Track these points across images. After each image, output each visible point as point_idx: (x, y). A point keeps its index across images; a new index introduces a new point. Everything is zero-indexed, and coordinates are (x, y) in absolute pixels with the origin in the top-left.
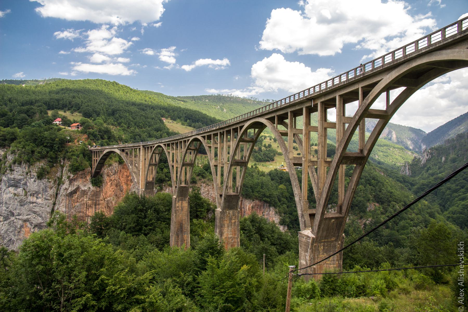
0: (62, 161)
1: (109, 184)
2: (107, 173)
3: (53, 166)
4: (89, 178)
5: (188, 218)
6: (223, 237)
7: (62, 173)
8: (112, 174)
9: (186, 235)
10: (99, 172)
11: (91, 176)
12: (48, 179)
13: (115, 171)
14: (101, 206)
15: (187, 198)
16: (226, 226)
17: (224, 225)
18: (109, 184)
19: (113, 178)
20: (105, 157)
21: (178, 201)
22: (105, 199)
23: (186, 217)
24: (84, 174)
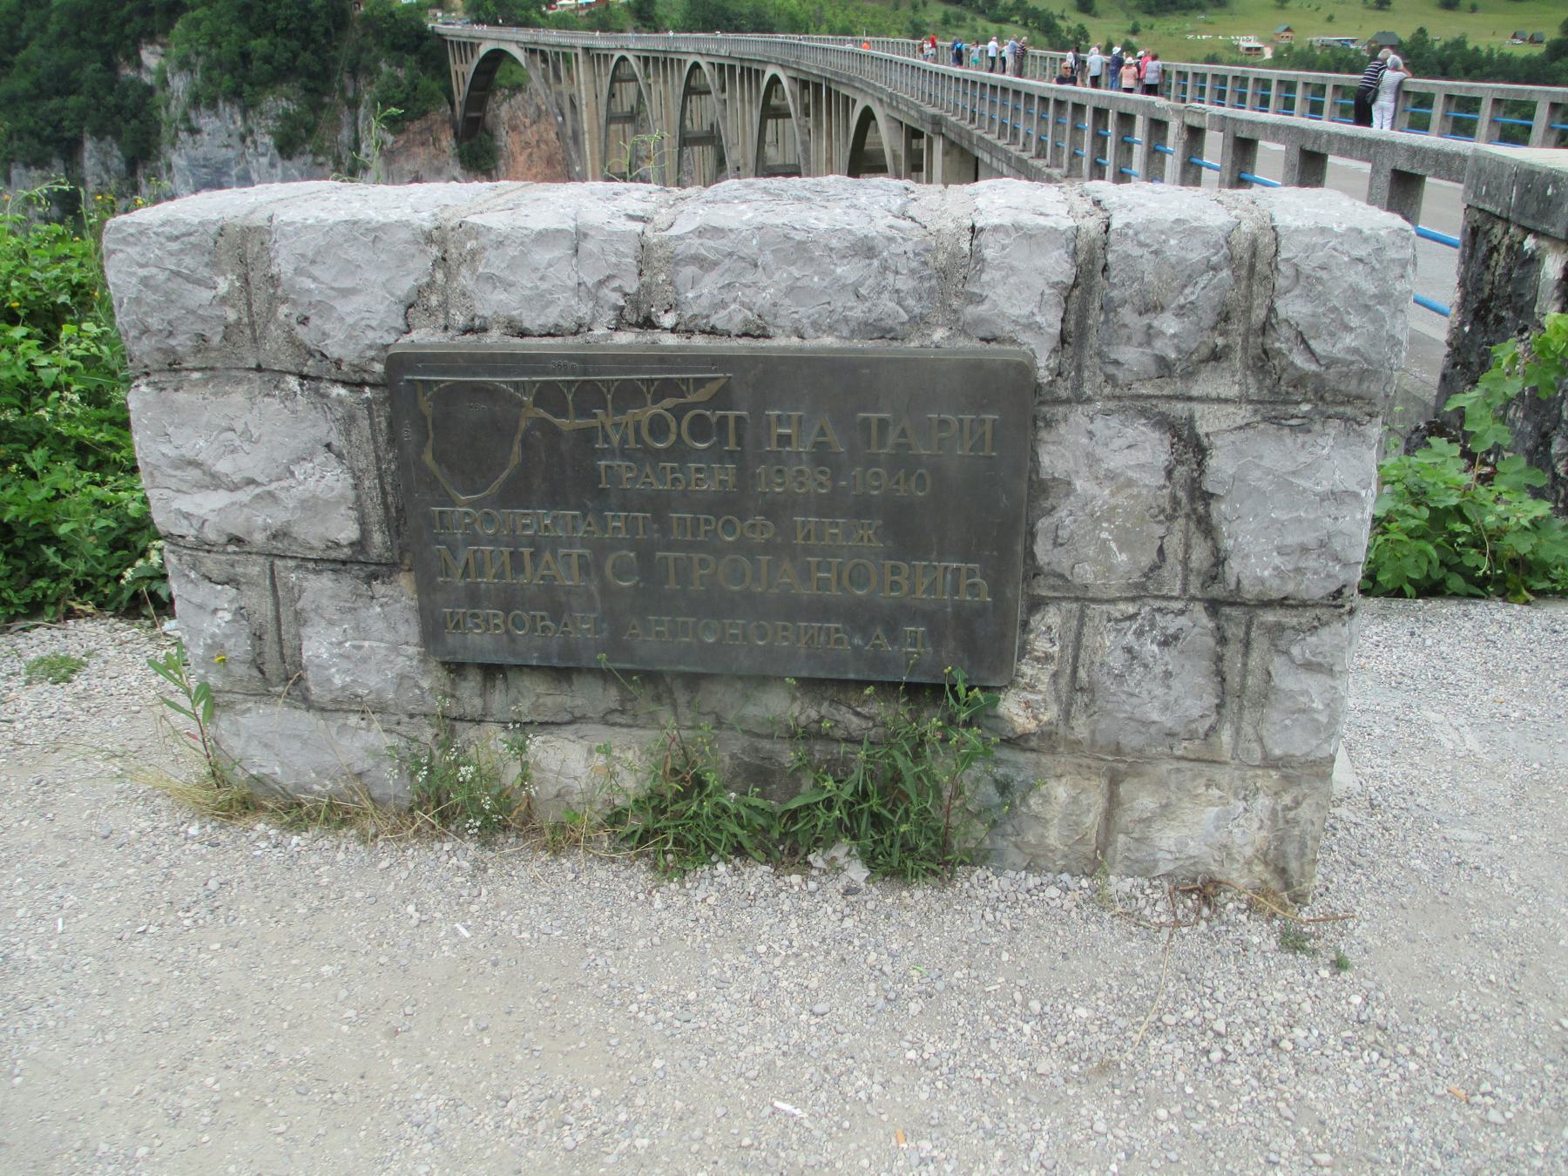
0: (347, 81)
1: (522, 159)
2: (511, 119)
3: (323, 106)
4: (447, 141)
7: (357, 132)
8: (528, 122)
10: (478, 119)
11: (456, 134)
12: (315, 154)
13: (538, 108)
18: (522, 159)
19: (530, 135)
24: (430, 129)
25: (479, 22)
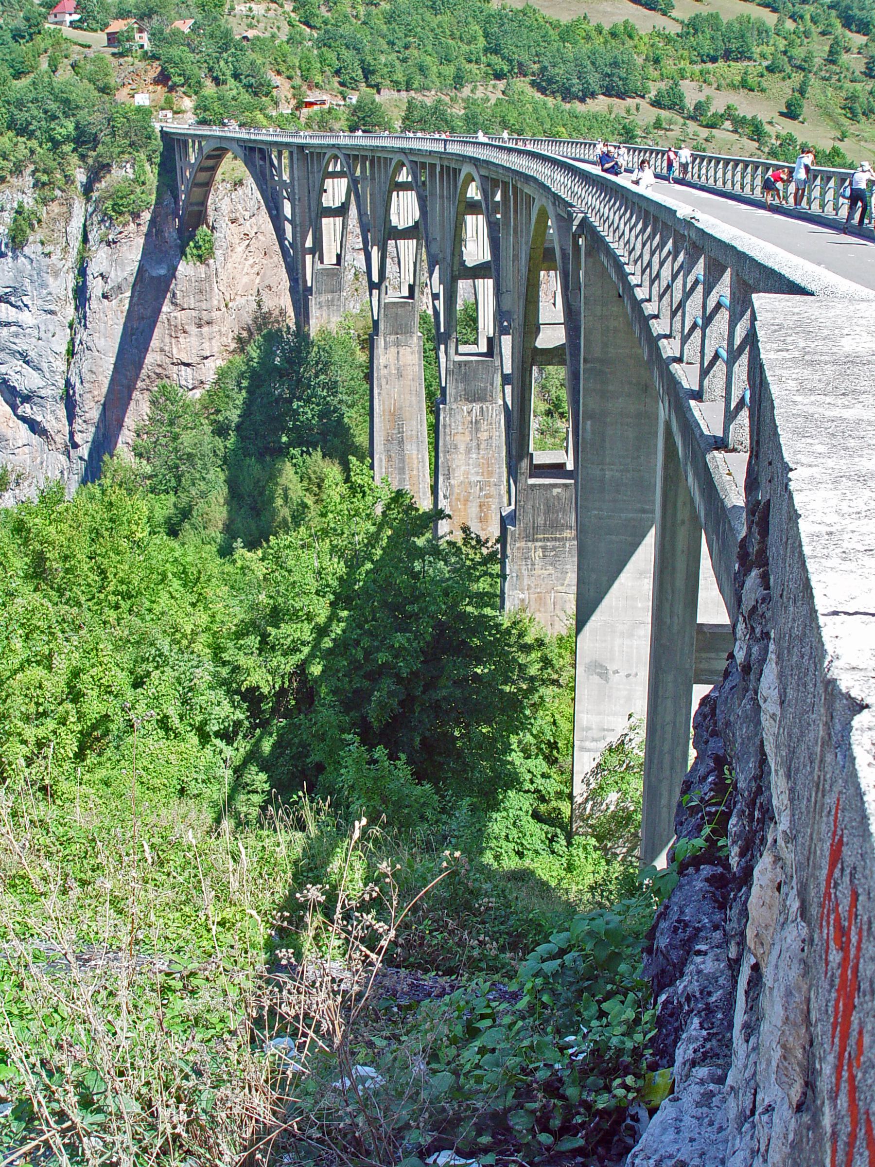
5: (419, 402)
6: (452, 481)
8: (247, 215)
9: (415, 452)
14: (215, 328)
15: (415, 339)
16: (461, 450)
17: (456, 447)
18: (240, 249)
20: (211, 163)
21: (386, 348)
22: (230, 305)
23: (414, 398)
25: (203, 122)
